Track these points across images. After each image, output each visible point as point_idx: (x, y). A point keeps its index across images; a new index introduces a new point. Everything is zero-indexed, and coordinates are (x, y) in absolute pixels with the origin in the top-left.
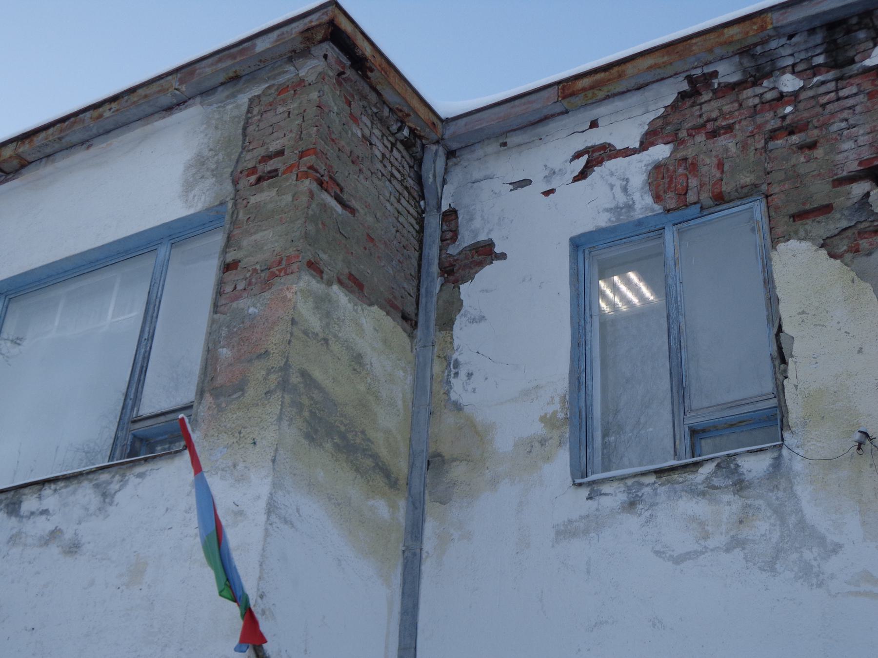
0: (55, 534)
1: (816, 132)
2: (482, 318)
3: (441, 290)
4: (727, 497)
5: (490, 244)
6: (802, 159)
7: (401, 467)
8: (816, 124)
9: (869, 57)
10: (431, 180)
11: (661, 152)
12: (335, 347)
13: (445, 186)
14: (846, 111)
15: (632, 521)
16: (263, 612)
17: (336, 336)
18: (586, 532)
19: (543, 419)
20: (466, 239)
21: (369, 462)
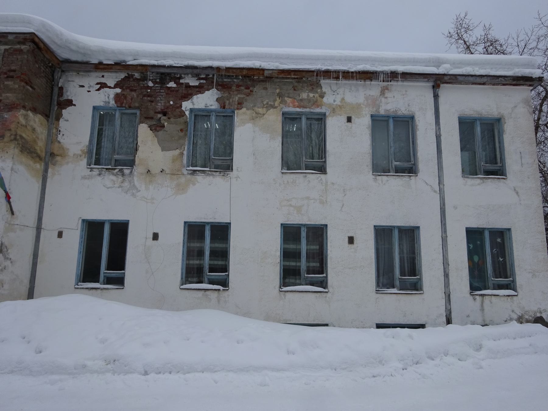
1: (154, 98)
2: (67, 121)
3: (57, 109)
4: (120, 177)
6: (150, 104)
7: (43, 155)
8: (154, 96)
9: (168, 84)
10: (56, 78)
11: (118, 90)
12: (29, 127)
13: (60, 80)
14: (161, 96)
15: (99, 178)
16: (10, 193)
17: (29, 125)
18: (89, 179)
19: (81, 150)
20: (65, 97)
21: (35, 155)
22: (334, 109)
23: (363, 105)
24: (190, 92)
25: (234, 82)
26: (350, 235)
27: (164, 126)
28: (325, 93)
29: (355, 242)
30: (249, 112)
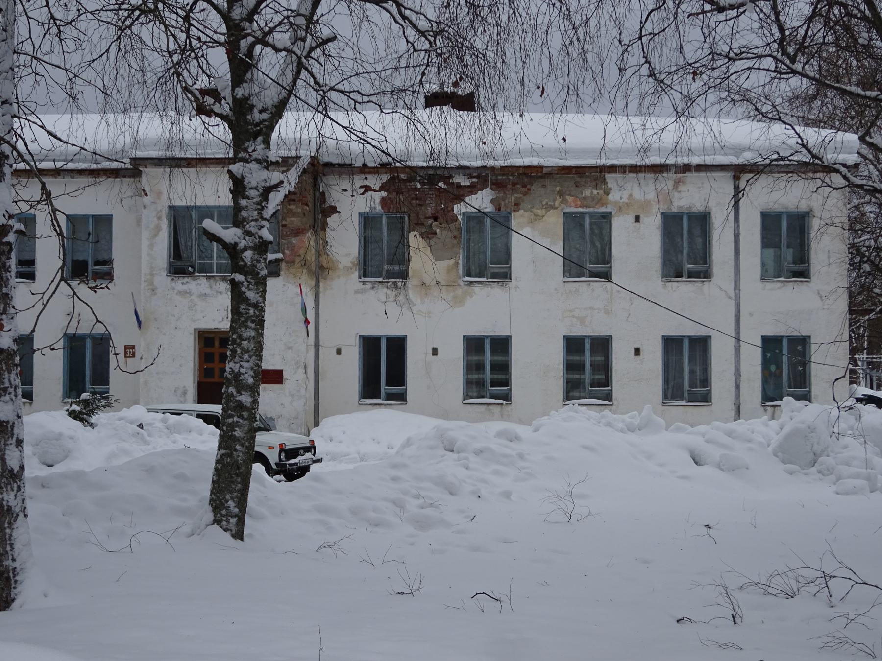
5: (335, 208)
11: (384, 194)
15: (372, 292)
18: (362, 293)
19: (351, 263)
22: (620, 208)
23: (653, 201)
24: (461, 193)
25: (510, 179)
26: (637, 346)
27: (435, 233)
28: (610, 189)
29: (641, 354)
30: (527, 214)
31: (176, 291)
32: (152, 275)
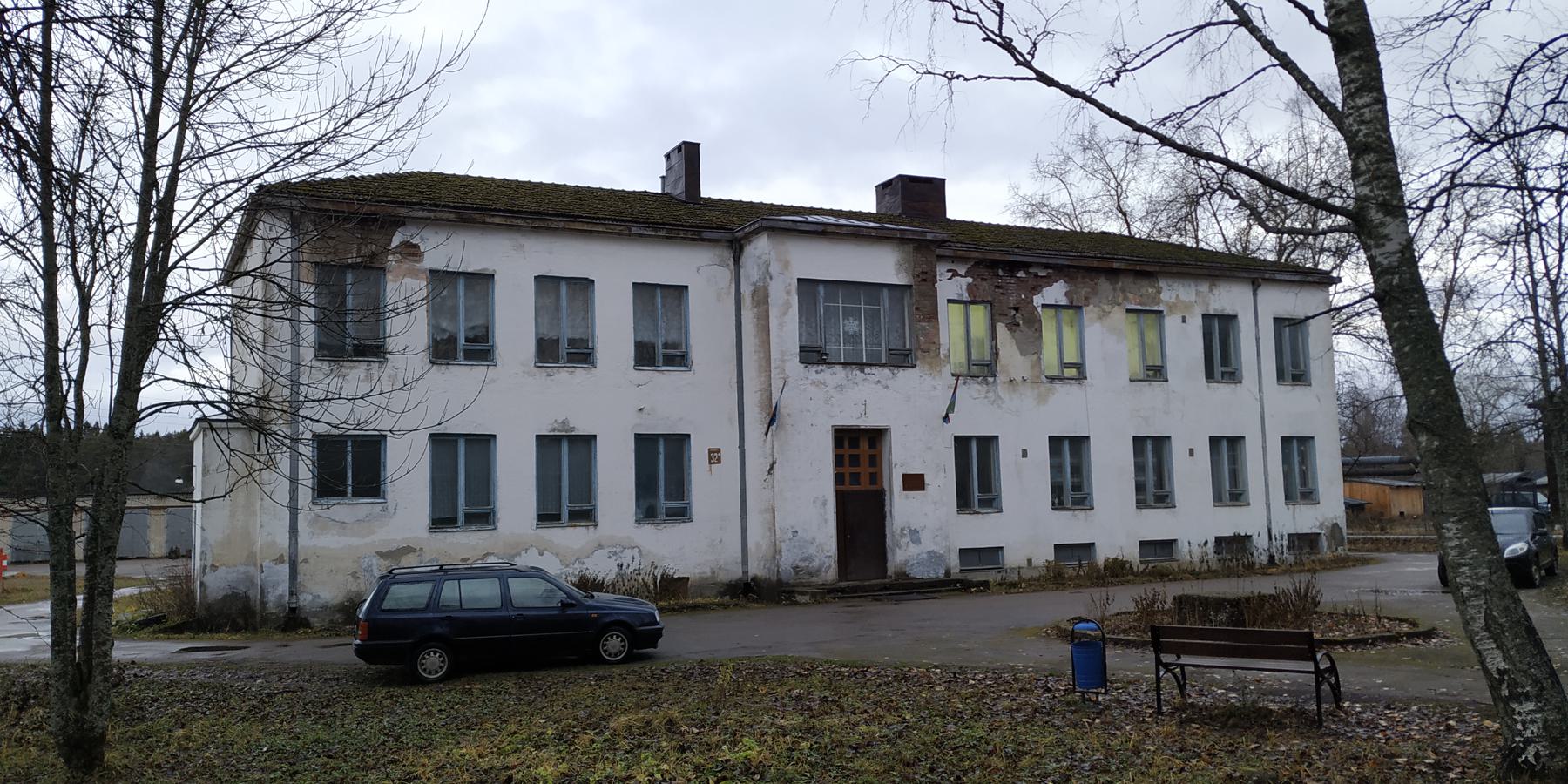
0: (879, 382)
11: (970, 280)
27: (1019, 325)
30: (1096, 309)
31: (810, 381)
32: (783, 361)
